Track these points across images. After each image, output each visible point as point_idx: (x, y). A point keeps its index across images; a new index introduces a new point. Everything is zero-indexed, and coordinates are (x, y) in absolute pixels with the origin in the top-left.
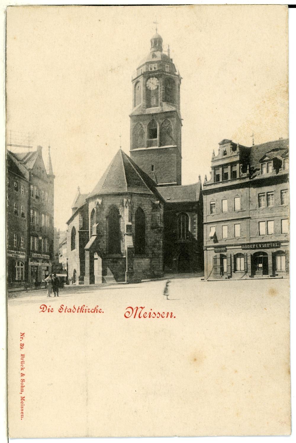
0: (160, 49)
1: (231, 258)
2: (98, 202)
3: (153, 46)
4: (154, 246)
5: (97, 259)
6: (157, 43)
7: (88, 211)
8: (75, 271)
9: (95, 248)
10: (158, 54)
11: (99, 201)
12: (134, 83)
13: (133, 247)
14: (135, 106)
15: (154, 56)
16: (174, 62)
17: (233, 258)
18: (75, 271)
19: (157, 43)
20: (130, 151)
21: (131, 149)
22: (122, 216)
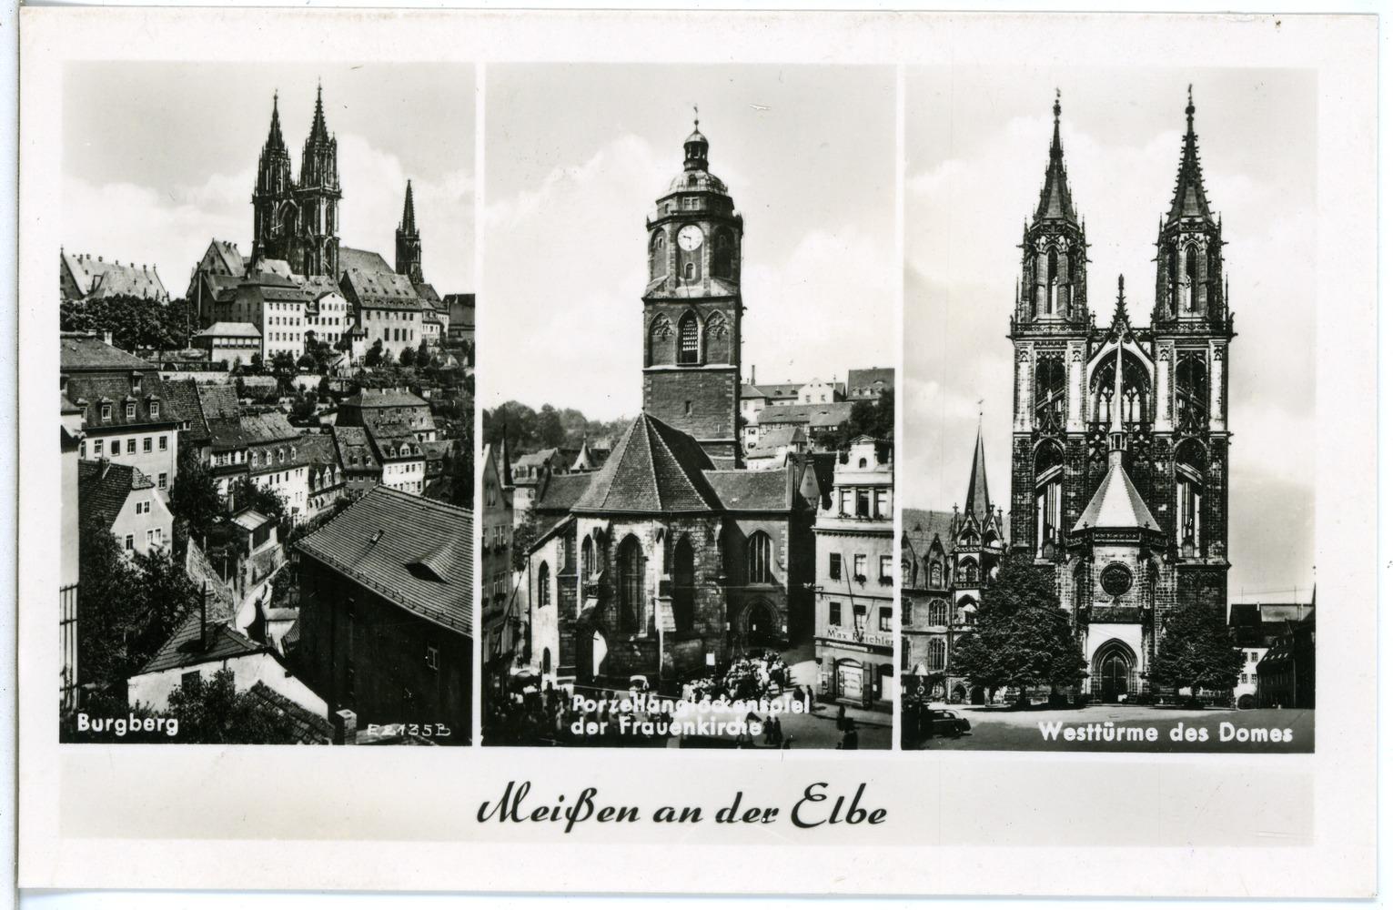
0: (703, 165)
1: (871, 671)
3: (689, 156)
4: (711, 615)
6: (697, 152)
7: (575, 535)
8: (547, 652)
10: (700, 174)
11: (603, 524)
13: (674, 630)
14: (652, 278)
15: (693, 181)
16: (730, 193)
17: (874, 673)
18: (547, 652)
19: (697, 152)
22: (650, 558)
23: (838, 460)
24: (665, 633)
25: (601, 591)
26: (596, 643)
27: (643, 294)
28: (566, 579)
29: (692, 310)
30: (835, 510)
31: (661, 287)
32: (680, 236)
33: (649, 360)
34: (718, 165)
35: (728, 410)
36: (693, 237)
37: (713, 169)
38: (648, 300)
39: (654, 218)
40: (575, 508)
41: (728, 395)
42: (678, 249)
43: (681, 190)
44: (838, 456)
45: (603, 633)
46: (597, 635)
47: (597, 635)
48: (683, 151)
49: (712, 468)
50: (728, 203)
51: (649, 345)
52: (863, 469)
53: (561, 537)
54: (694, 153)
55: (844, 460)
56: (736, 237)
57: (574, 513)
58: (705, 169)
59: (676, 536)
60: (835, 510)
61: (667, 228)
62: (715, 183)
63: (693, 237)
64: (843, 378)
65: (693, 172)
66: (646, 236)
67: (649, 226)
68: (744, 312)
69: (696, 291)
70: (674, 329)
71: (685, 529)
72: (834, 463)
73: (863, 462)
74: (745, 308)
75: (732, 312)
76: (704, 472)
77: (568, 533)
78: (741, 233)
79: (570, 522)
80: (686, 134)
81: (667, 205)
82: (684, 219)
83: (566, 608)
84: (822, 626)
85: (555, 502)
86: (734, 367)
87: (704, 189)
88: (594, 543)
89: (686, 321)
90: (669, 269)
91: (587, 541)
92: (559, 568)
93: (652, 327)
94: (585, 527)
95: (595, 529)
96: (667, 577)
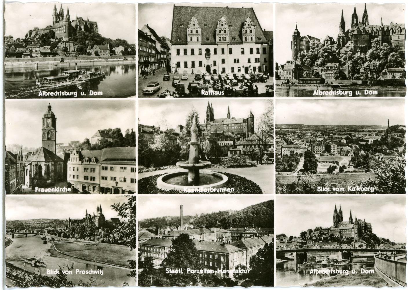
0: (50, 110)
11: (36, 163)
15: (49, 112)
25: (36, 174)
28: (31, 171)
33: (43, 139)
34: (53, 110)
36: (50, 121)
42: (47, 123)
50: (54, 116)
51: (43, 136)
62: (52, 112)
64: (70, 143)
69: (50, 129)
70: (46, 134)
73: (74, 154)
77: (31, 164)
80: (48, 105)
82: (48, 118)
83: (30, 176)
85: (28, 160)
89: (48, 133)
90: (45, 126)
93: (44, 134)
94: (33, 163)
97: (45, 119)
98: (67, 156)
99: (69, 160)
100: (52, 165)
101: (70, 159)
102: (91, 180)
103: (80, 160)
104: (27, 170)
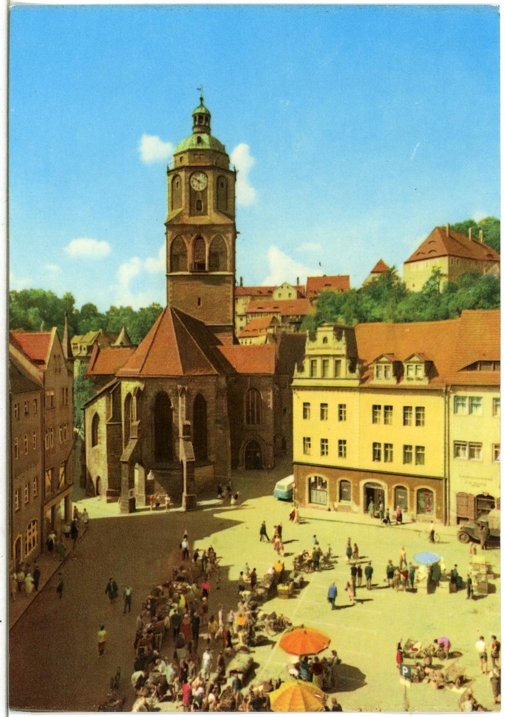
0: (207, 130)
2: (139, 388)
3: (197, 123)
5: (137, 469)
6: (202, 121)
9: (136, 459)
10: (205, 137)
11: (141, 386)
12: (172, 177)
13: (194, 460)
15: (199, 140)
19: (202, 121)
20: (167, 276)
21: (167, 272)
23: (308, 339)
24: (187, 463)
26: (137, 472)
27: (165, 222)
29: (199, 232)
30: (307, 373)
31: (178, 217)
32: (192, 180)
34: (218, 129)
35: (228, 304)
37: (213, 133)
38: (169, 225)
39: (172, 167)
40: (118, 374)
41: (227, 294)
43: (191, 148)
44: (308, 335)
45: (141, 463)
46: (137, 465)
47: (137, 465)
48: (192, 119)
49: (222, 345)
52: (325, 345)
53: (108, 395)
54: (200, 122)
55: (313, 338)
56: (231, 182)
57: (119, 378)
58: (209, 134)
59: (194, 393)
60: (307, 373)
61: (182, 174)
62: (215, 142)
63: (202, 182)
65: (199, 135)
66: (167, 180)
67: (169, 172)
68: (238, 235)
71: (200, 387)
72: (305, 341)
74: (239, 233)
75: (230, 236)
76: (219, 347)
77: (114, 393)
78: (235, 180)
79: (115, 384)
81: (181, 159)
82: (193, 170)
84: (298, 455)
86: (231, 273)
87: (208, 147)
88: (134, 398)
91: (129, 396)
92: (107, 418)
95: (135, 389)
96: (188, 423)
97: (182, 174)
98: (290, 353)
99: (301, 369)
100: (219, 393)
101: (307, 363)
102: (407, 458)
103: (352, 369)
104: (96, 418)
